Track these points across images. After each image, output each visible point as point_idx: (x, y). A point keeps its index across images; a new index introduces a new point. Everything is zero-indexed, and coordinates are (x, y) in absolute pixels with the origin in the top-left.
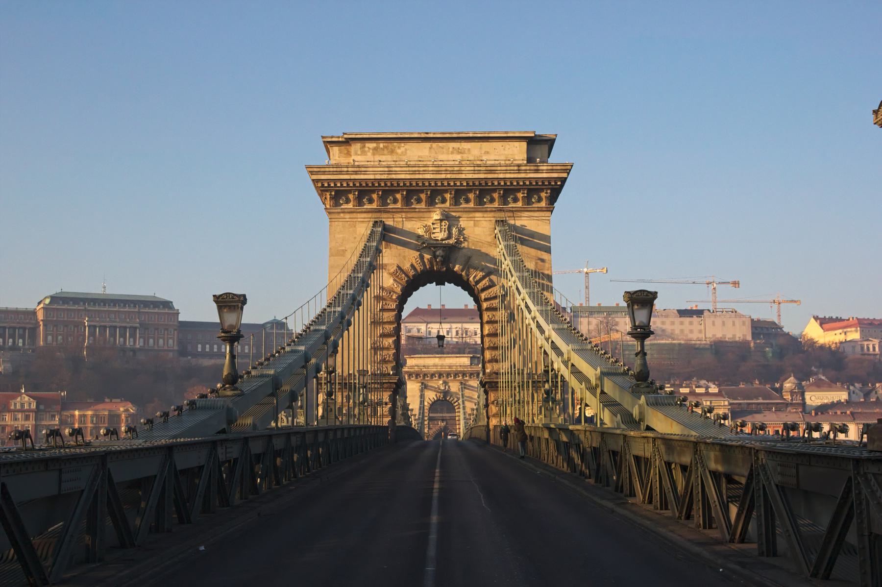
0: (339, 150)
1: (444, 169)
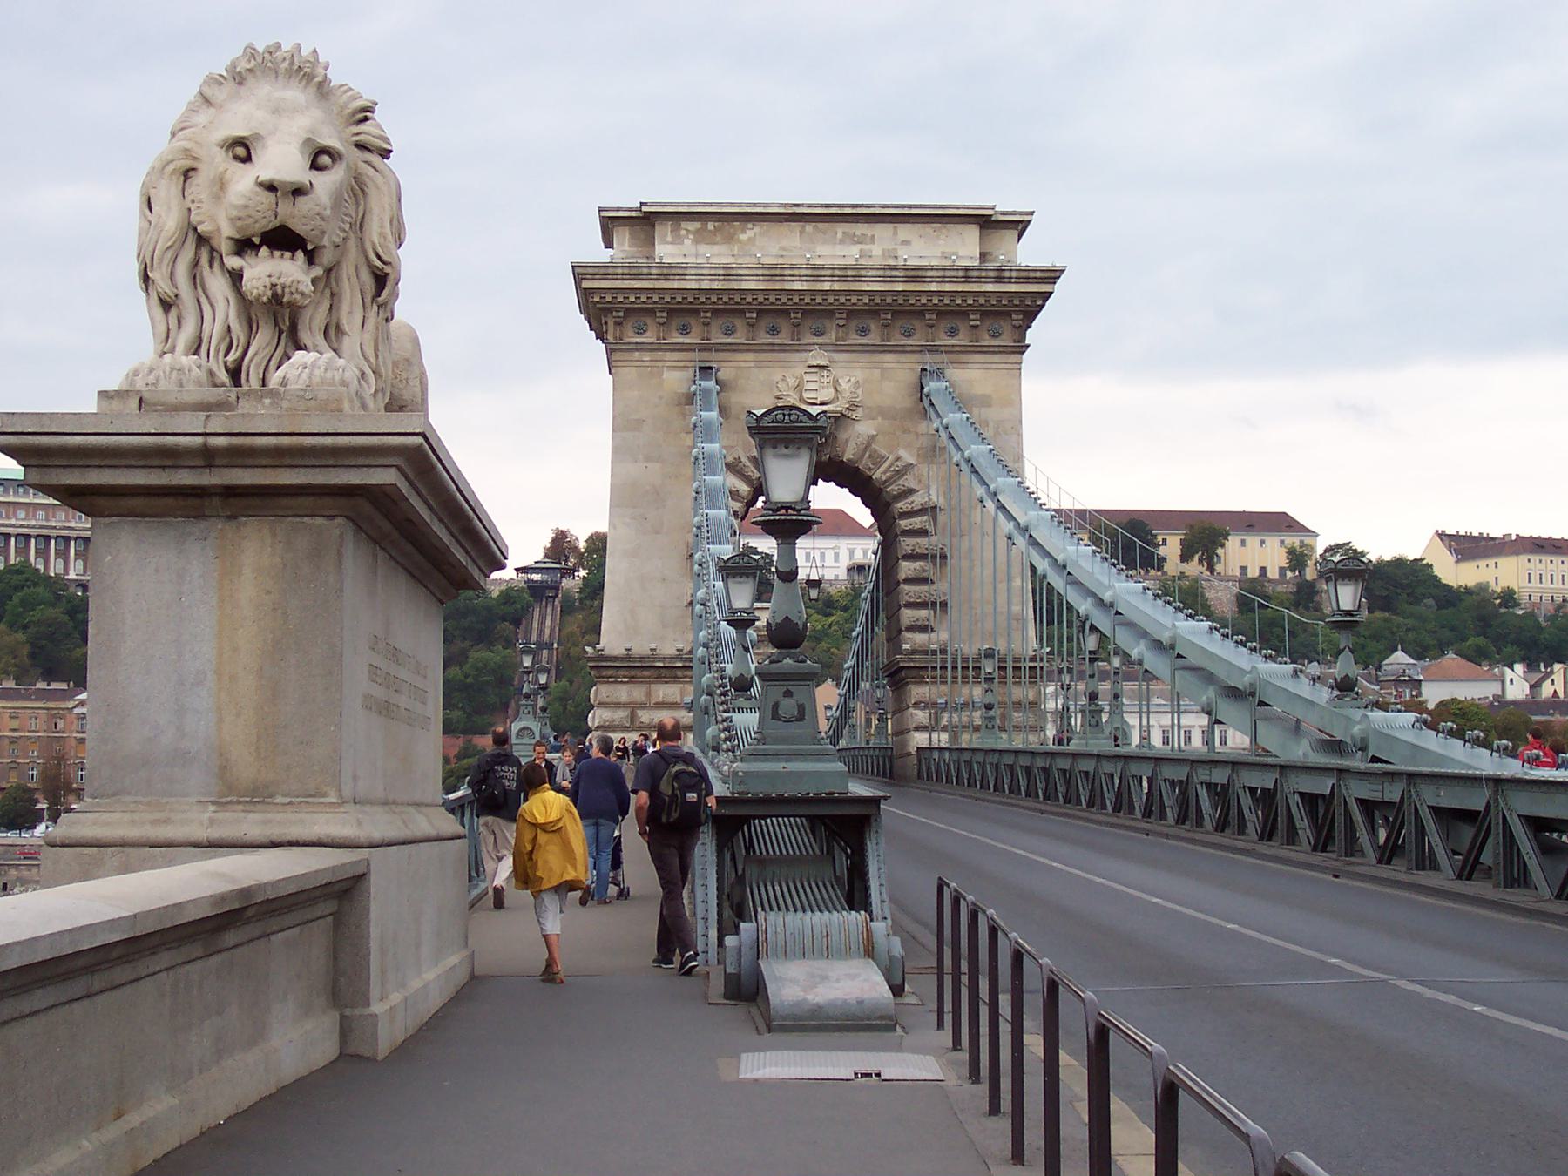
0: (632, 236)
1: (829, 272)
